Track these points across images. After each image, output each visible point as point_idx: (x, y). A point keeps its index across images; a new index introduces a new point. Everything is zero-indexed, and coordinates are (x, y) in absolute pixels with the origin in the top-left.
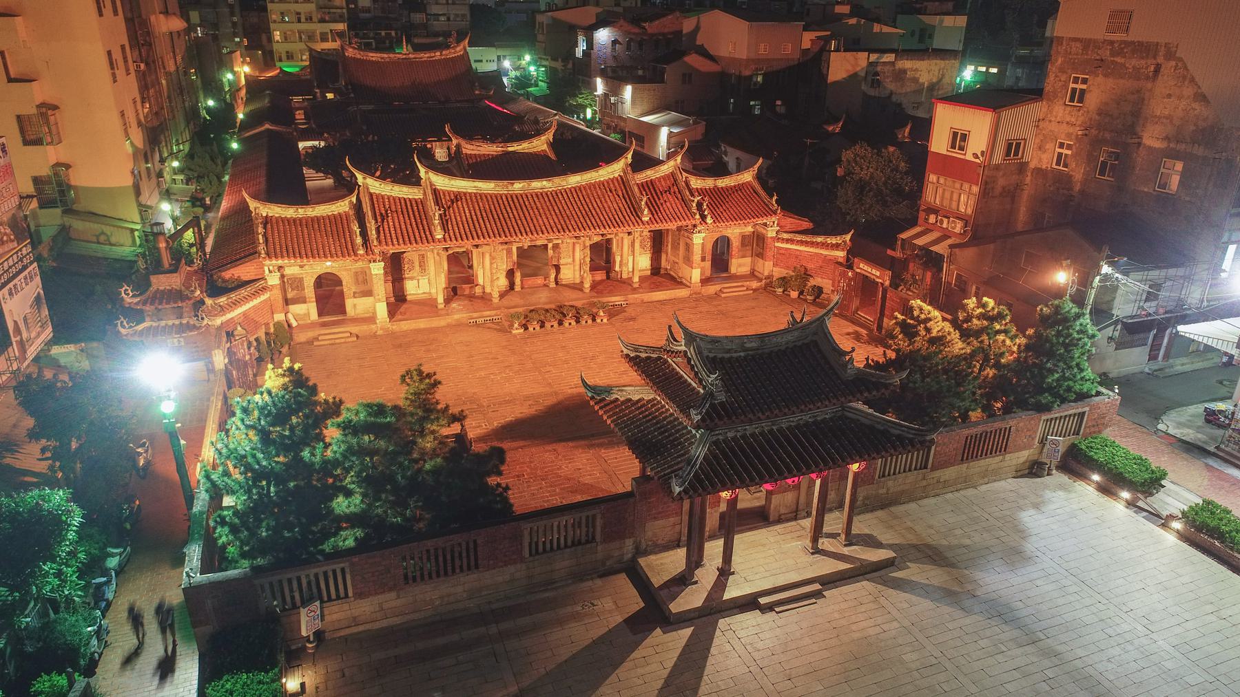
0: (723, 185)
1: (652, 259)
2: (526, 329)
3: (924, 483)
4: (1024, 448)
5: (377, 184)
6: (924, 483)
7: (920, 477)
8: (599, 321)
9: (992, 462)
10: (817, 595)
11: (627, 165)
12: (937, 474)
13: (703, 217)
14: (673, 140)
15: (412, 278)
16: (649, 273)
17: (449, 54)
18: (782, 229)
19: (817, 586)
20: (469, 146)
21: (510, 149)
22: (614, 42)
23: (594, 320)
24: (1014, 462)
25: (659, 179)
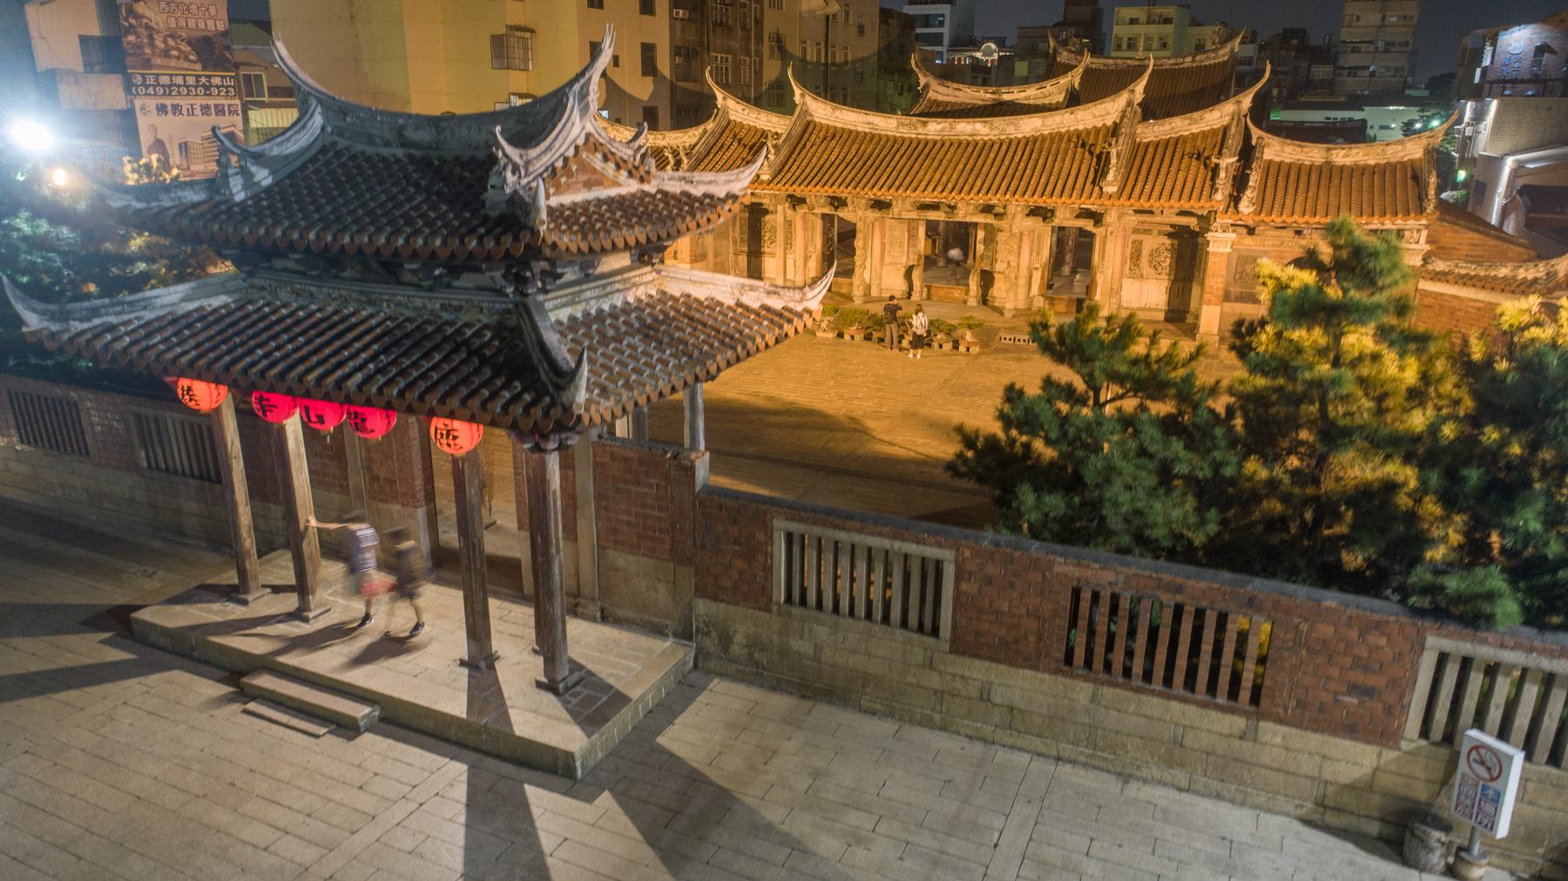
0: (1348, 161)
1: (1171, 292)
2: (841, 335)
3: (933, 680)
4: (1351, 729)
5: (739, 108)
6: (933, 680)
7: (918, 655)
8: (962, 349)
9: (1213, 725)
10: (346, 728)
11: (1130, 103)
12: (978, 670)
13: (1235, 199)
14: (1521, 182)
15: (773, 255)
16: (1161, 316)
17: (1357, 115)
18: (1438, 249)
19: (360, 711)
20: (941, 89)
21: (1006, 97)
22: (1541, 50)
23: (956, 347)
24: (1307, 766)
25: (1194, 136)
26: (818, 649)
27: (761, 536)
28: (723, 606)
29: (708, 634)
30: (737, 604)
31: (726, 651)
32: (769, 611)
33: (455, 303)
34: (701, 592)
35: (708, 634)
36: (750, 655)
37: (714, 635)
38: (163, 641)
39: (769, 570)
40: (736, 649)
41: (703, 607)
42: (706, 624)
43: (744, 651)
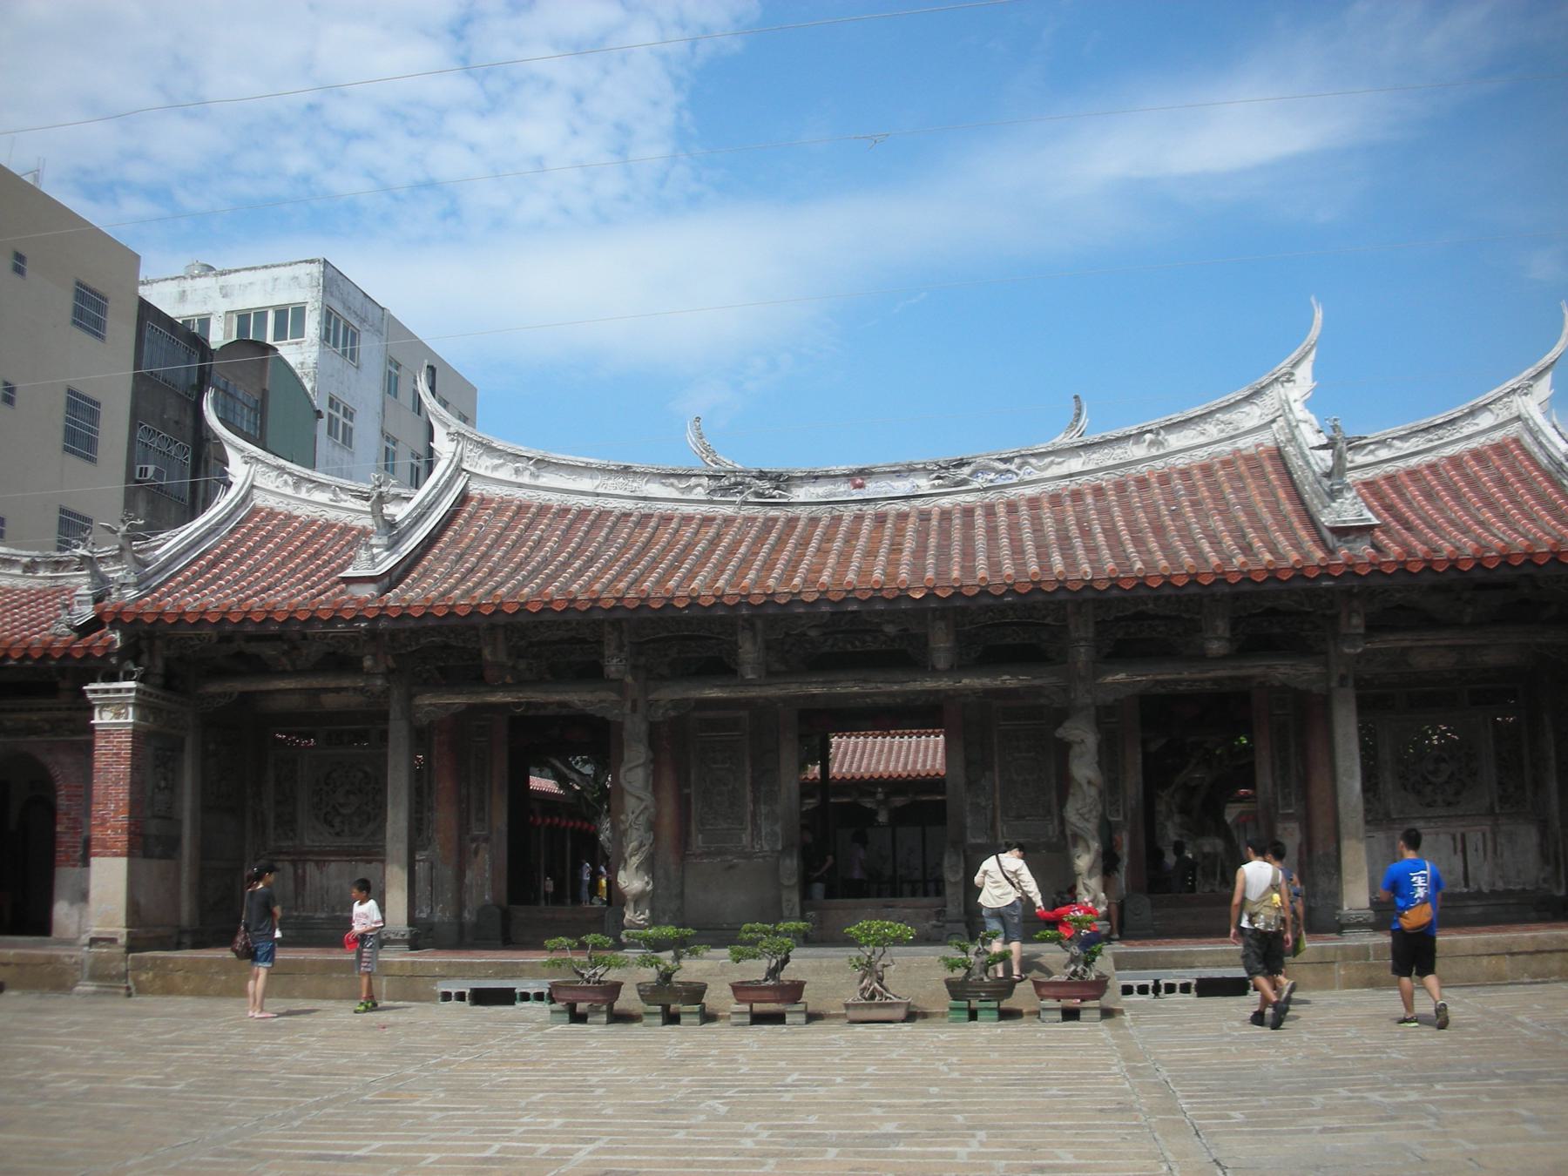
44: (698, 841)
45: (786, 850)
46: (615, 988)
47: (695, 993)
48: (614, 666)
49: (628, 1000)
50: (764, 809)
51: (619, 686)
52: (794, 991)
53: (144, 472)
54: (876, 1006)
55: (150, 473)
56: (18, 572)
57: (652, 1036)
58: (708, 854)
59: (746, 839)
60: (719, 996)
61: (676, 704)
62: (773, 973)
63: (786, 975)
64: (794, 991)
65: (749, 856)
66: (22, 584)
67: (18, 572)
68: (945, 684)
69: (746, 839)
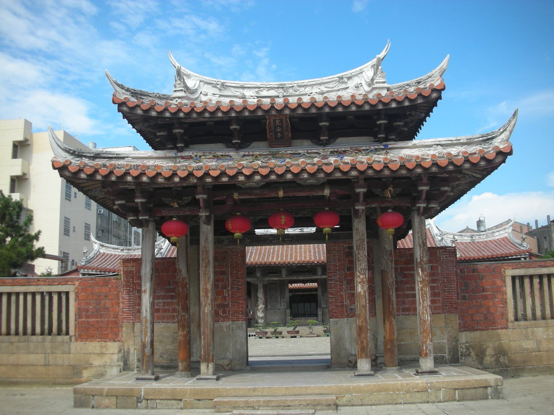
26: (539, 342)
27: (499, 282)
28: (477, 333)
29: (469, 355)
30: (487, 329)
31: (481, 363)
32: (506, 328)
33: (343, 149)
34: (465, 327)
35: (469, 355)
36: (497, 360)
37: (473, 354)
38: (106, 401)
39: (505, 302)
40: (488, 359)
41: (465, 337)
42: (467, 348)
43: (493, 359)
44: (269, 307)
45: (287, 308)
46: (267, 333)
47: (281, 333)
48: (258, 274)
49: (269, 335)
50: (282, 300)
51: (258, 278)
52: (298, 332)
53: (100, 211)
54: (311, 335)
55: (102, 212)
56: (119, 251)
57: (274, 340)
58: (271, 309)
59: (279, 306)
60: (285, 333)
61: (268, 281)
62: (294, 329)
63: (297, 329)
64: (298, 332)
65: (279, 310)
66: (121, 254)
67: (119, 251)
68: (319, 277)
69: (279, 306)
